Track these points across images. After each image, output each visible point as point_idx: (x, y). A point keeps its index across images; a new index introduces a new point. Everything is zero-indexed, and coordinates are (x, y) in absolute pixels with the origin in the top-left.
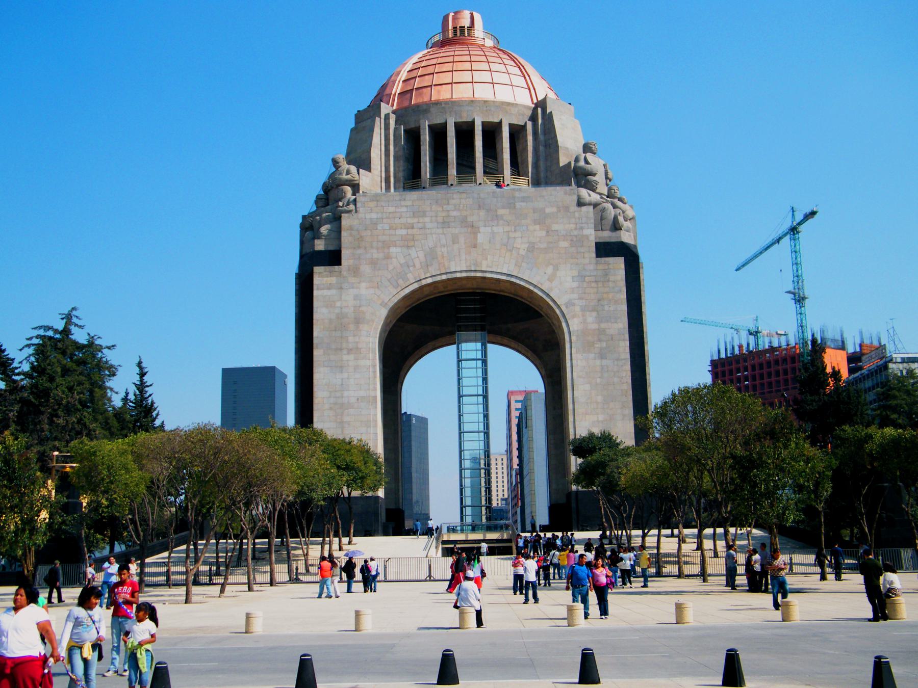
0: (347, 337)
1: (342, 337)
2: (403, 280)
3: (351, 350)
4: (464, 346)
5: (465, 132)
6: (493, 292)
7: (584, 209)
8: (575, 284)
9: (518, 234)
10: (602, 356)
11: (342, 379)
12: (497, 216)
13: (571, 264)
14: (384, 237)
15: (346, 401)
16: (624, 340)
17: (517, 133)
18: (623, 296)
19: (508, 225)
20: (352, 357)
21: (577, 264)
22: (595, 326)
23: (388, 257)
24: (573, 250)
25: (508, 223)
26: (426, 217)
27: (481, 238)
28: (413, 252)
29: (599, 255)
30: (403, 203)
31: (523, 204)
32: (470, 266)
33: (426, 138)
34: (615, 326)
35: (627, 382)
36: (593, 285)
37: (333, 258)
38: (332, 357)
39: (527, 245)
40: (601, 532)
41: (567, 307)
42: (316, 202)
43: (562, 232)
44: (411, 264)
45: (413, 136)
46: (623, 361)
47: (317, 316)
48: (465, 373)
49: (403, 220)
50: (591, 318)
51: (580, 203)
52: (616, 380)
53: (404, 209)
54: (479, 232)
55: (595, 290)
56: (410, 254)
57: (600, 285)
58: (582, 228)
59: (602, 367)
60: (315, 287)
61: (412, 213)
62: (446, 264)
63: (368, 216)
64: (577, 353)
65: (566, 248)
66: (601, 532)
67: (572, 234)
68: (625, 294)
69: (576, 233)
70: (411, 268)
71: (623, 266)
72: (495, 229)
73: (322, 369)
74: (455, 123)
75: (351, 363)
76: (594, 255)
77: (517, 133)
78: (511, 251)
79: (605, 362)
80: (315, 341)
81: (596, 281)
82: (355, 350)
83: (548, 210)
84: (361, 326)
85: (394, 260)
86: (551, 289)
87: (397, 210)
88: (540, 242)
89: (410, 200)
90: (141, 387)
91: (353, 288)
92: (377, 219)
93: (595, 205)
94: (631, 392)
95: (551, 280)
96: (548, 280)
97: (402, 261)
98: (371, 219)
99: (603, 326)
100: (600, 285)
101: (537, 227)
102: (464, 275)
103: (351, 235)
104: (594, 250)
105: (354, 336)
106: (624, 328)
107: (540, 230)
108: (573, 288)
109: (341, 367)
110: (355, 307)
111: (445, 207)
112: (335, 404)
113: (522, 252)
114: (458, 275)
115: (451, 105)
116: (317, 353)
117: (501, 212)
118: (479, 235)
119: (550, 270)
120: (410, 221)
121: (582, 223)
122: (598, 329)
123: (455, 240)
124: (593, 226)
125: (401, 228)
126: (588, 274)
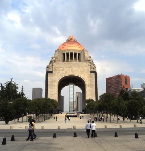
4: (71, 86)
5: (71, 54)
10: (91, 87)
17: (79, 54)
20: (54, 87)
22: (90, 83)
23: (60, 72)
25: (78, 68)
27: (73, 70)
37: (51, 72)
45: (64, 54)
47: (48, 81)
48: (70, 90)
79: (92, 89)
82: (55, 86)
90: (22, 91)
93: (91, 65)
95: (84, 76)
115: (69, 50)
116: (48, 86)
117: (77, 66)
119: (84, 75)
123: (70, 70)
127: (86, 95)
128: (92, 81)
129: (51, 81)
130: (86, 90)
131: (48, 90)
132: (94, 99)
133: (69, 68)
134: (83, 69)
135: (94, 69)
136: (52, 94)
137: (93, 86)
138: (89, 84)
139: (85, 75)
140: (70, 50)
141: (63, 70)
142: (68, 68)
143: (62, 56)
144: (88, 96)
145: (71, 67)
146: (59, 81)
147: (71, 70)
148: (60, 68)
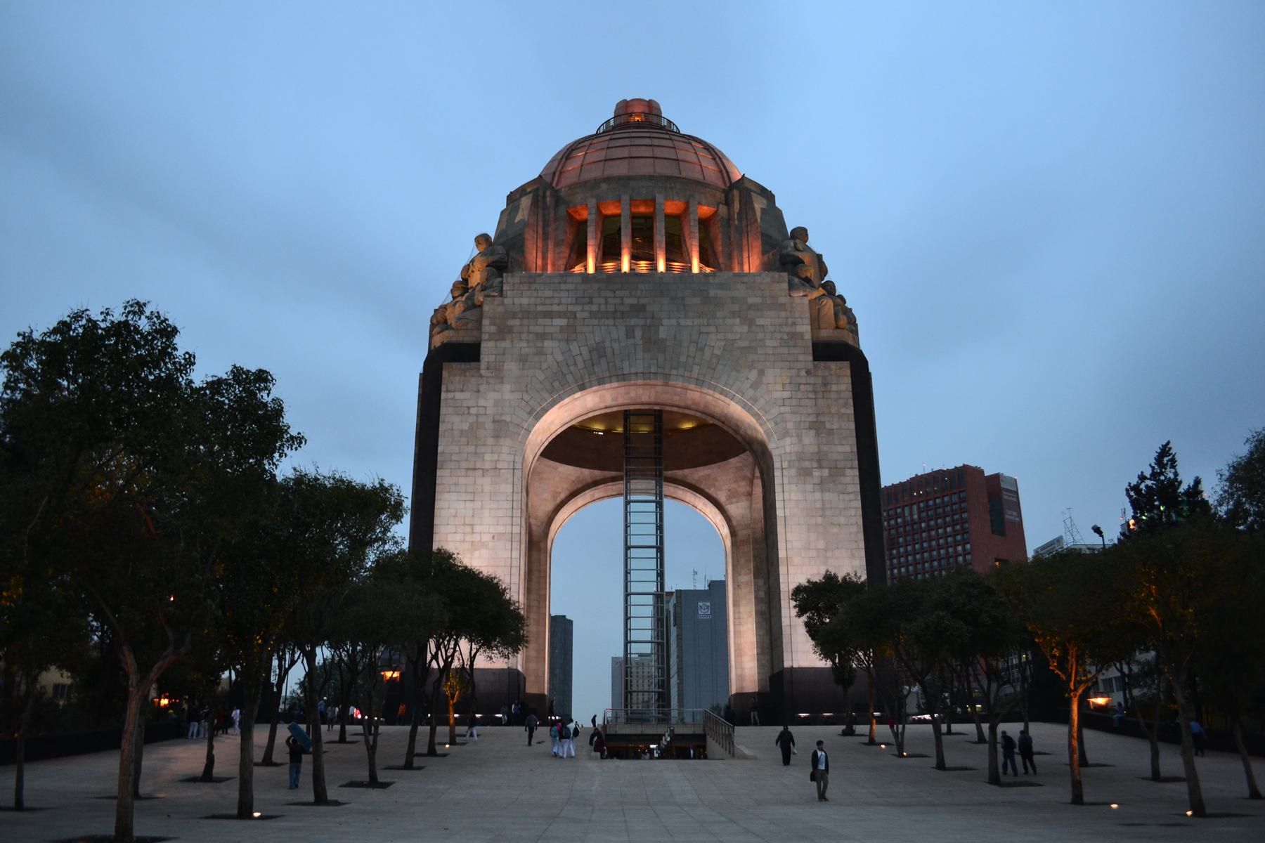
0: (484, 453)
1: (475, 453)
2: (560, 383)
3: (487, 470)
6: (675, 409)
8: (787, 394)
9: (712, 329)
11: (474, 509)
12: (684, 305)
13: (782, 368)
14: (537, 327)
15: (478, 539)
16: (852, 468)
19: (699, 317)
21: (790, 368)
22: (814, 449)
23: (541, 352)
24: (785, 350)
26: (592, 304)
27: (663, 333)
28: (574, 347)
29: (816, 358)
30: (563, 286)
31: (720, 293)
32: (650, 367)
35: (857, 523)
39: (723, 343)
40: (844, 727)
42: (452, 291)
43: (769, 327)
46: (852, 496)
49: (562, 308)
50: (809, 439)
53: (563, 294)
54: (662, 325)
56: (570, 350)
57: (820, 395)
58: (794, 324)
60: (443, 388)
61: (574, 299)
63: (517, 301)
65: (774, 347)
66: (844, 727)
67: (782, 330)
68: (852, 408)
69: (787, 329)
70: (572, 368)
71: (848, 372)
72: (682, 322)
75: (487, 488)
76: (810, 358)
78: (702, 350)
79: (827, 496)
81: (815, 392)
83: (751, 300)
84: (502, 440)
85: (550, 358)
87: (556, 295)
88: (740, 339)
89: (572, 283)
91: (494, 391)
92: (529, 304)
94: (861, 536)
96: (751, 387)
97: (560, 358)
98: (521, 305)
99: (825, 448)
100: (820, 395)
101: (737, 321)
103: (492, 324)
104: (810, 350)
106: (852, 452)
108: (784, 399)
111: (617, 292)
112: (464, 541)
118: (661, 328)
120: (571, 308)
121: (795, 318)
122: (818, 453)
124: (808, 321)
125: (560, 317)
126: (803, 380)
127: (782, 554)
129: (465, 426)
133: (624, 315)
134: (751, 323)
138: (801, 457)
140: (630, 178)
142: (615, 315)
145: (639, 309)
147: (638, 333)
148: (548, 315)
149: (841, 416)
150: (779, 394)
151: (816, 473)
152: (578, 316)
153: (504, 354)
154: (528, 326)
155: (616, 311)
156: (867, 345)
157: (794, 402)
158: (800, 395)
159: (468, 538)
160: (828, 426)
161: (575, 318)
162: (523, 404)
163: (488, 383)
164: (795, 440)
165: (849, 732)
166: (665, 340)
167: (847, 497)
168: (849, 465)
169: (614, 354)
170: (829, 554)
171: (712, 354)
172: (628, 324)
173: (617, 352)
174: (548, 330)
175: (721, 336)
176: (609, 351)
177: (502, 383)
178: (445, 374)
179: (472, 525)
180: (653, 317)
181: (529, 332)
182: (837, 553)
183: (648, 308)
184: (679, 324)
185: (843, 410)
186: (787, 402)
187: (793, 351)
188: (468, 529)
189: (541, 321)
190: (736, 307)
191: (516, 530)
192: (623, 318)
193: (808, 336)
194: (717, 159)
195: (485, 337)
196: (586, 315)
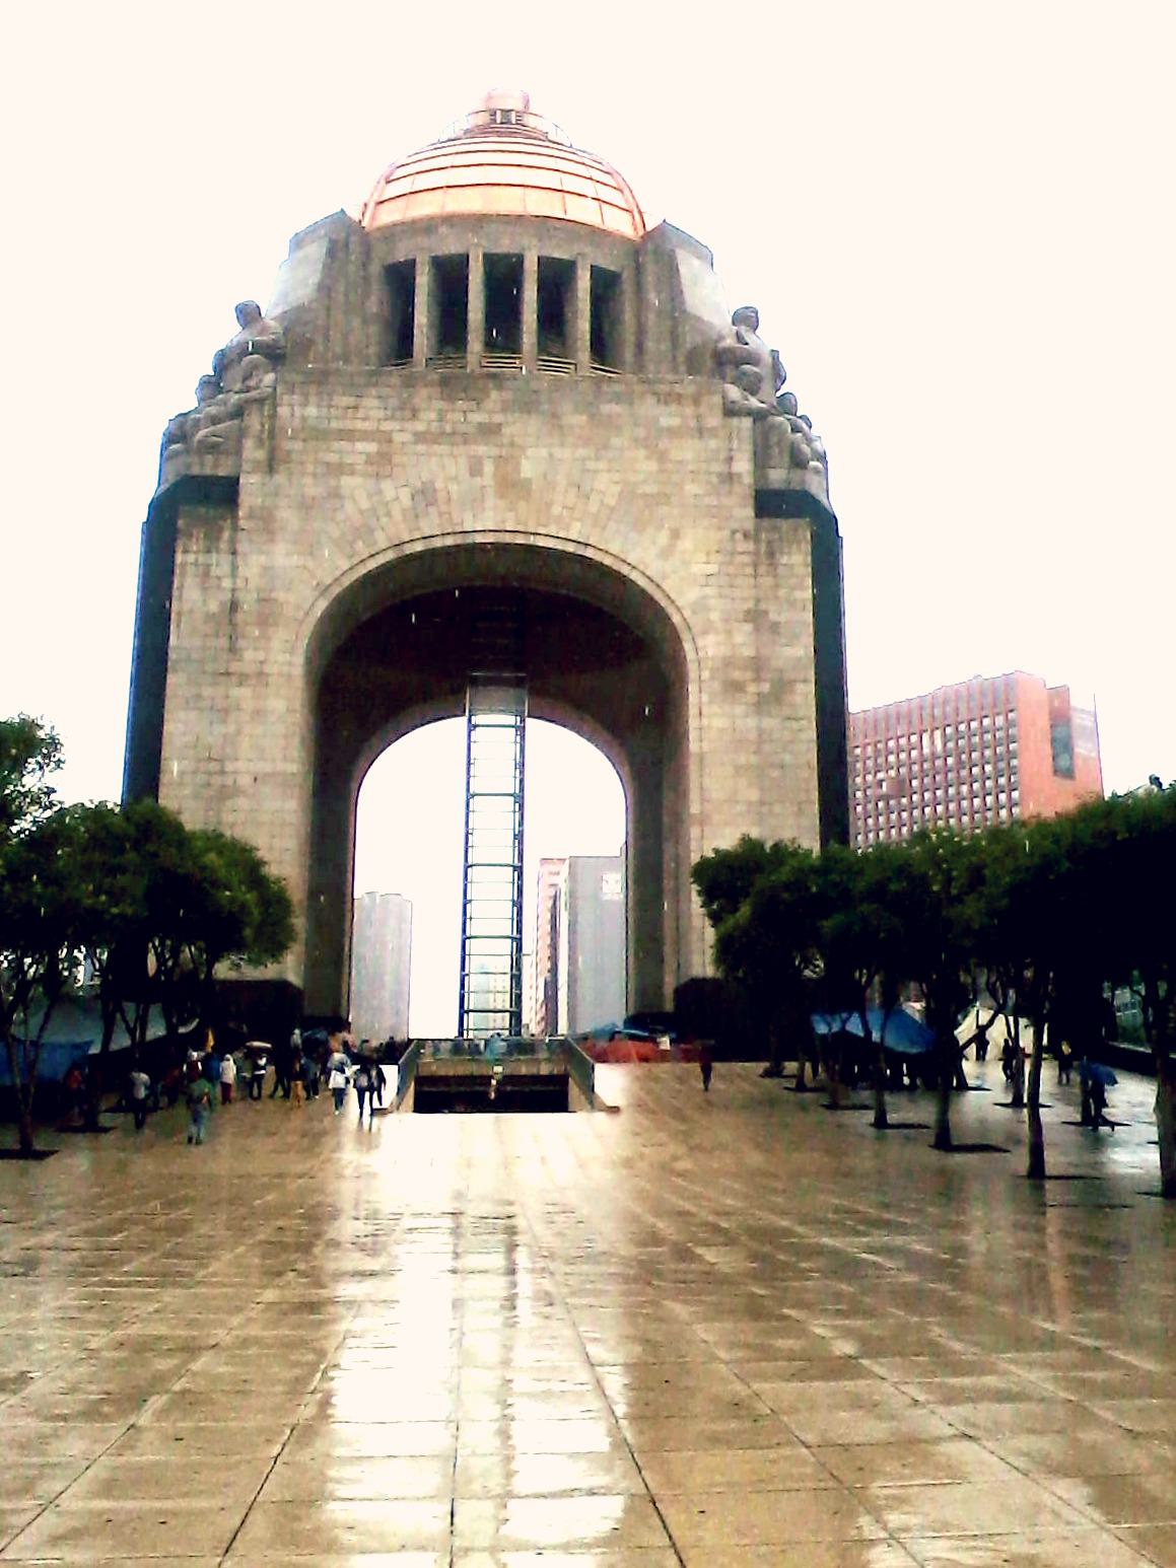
5: (504, 276)
7: (735, 421)
8: (712, 568)
9: (602, 465)
16: (805, 681)
17: (605, 285)
18: (807, 594)
22: (748, 652)
23: (335, 494)
27: (528, 469)
28: (388, 488)
33: (423, 281)
34: (788, 652)
36: (749, 570)
38: (207, 691)
41: (694, 612)
44: (381, 511)
45: (400, 278)
46: (804, 722)
50: (743, 635)
51: (730, 411)
52: (788, 758)
55: (752, 581)
56: (380, 492)
59: (761, 732)
62: (456, 518)
64: (711, 702)
66: (767, 1064)
70: (384, 520)
72: (558, 452)
73: (182, 715)
74: (485, 255)
75: (248, 705)
76: (750, 512)
77: (605, 285)
79: (769, 723)
80: (172, 655)
85: (349, 506)
86: (664, 577)
93: (759, 417)
95: (666, 553)
99: (765, 651)
101: (642, 453)
102: (490, 538)
105: (256, 649)
107: (648, 458)
109: (226, 711)
110: (259, 591)
113: (612, 502)
114: (479, 539)
119: (663, 538)
120: (387, 426)
123: (475, 470)
127: (695, 808)
128: (775, 628)
129: (213, 607)
130: (693, 746)
131: (169, 728)
132: (810, 842)
134: (662, 457)
135: (798, 462)
136: (225, 793)
137: (782, 688)
138: (728, 663)
139: (686, 543)
141: (382, 463)
143: (376, 301)
144: (716, 818)
146: (322, 605)
147: (489, 468)
149: (792, 604)
150: (699, 568)
151: (752, 688)
152: (398, 438)
153: (276, 494)
154: (316, 452)
155: (454, 433)
156: (842, 497)
157: (724, 580)
158: (731, 570)
159: (217, 780)
160: (773, 616)
161: (390, 441)
162: (306, 575)
163: (251, 541)
164: (721, 638)
165: (774, 1073)
166: (529, 481)
167: (795, 725)
168: (802, 677)
169: (449, 500)
170: (765, 809)
171: (602, 502)
172: (472, 453)
173: (454, 496)
174: (348, 460)
175: (617, 477)
176: (441, 496)
177: (272, 541)
178: (181, 523)
179: (220, 761)
180: (512, 444)
181: (316, 462)
182: (777, 808)
183: (506, 431)
184: (551, 455)
185: (798, 594)
186: (712, 580)
187: (725, 501)
188: (213, 766)
189: (336, 445)
190: (641, 432)
191: (294, 767)
192: (465, 442)
193: (748, 480)
194: (626, 191)
195: (246, 467)
196: (407, 437)
